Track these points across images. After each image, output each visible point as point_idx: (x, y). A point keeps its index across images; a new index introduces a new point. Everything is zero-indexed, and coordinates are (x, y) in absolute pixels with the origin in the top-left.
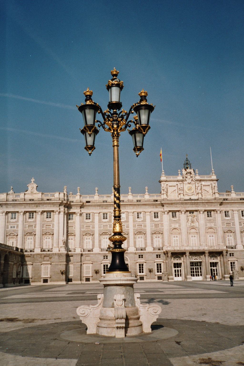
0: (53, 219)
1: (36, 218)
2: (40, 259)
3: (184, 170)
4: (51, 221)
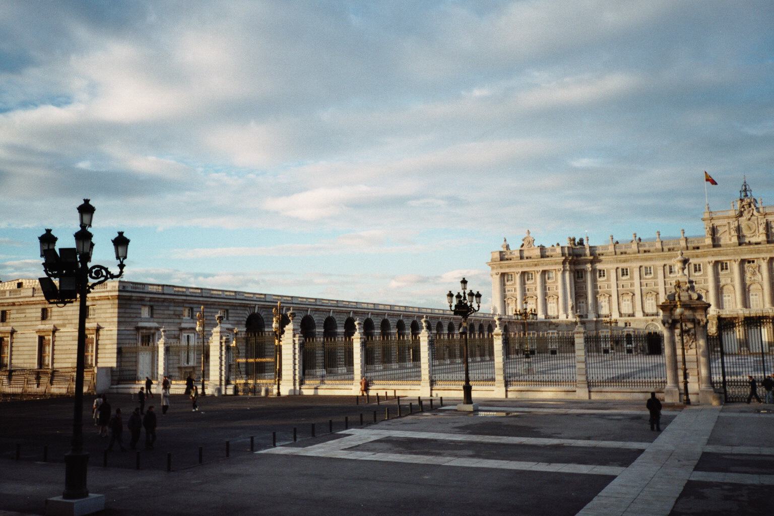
0: (556, 280)
1: (535, 279)
2: (544, 328)
3: (739, 202)
4: (554, 282)
